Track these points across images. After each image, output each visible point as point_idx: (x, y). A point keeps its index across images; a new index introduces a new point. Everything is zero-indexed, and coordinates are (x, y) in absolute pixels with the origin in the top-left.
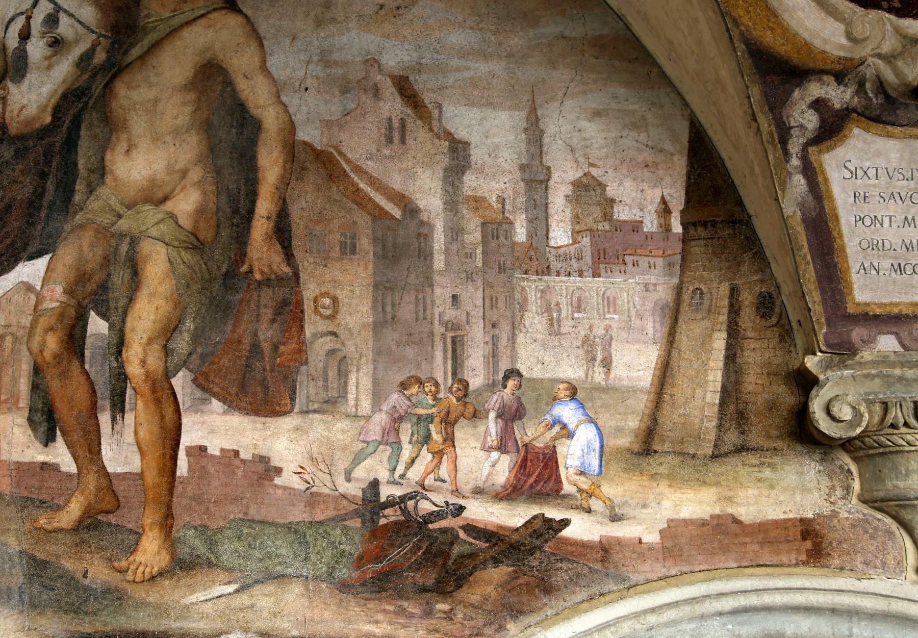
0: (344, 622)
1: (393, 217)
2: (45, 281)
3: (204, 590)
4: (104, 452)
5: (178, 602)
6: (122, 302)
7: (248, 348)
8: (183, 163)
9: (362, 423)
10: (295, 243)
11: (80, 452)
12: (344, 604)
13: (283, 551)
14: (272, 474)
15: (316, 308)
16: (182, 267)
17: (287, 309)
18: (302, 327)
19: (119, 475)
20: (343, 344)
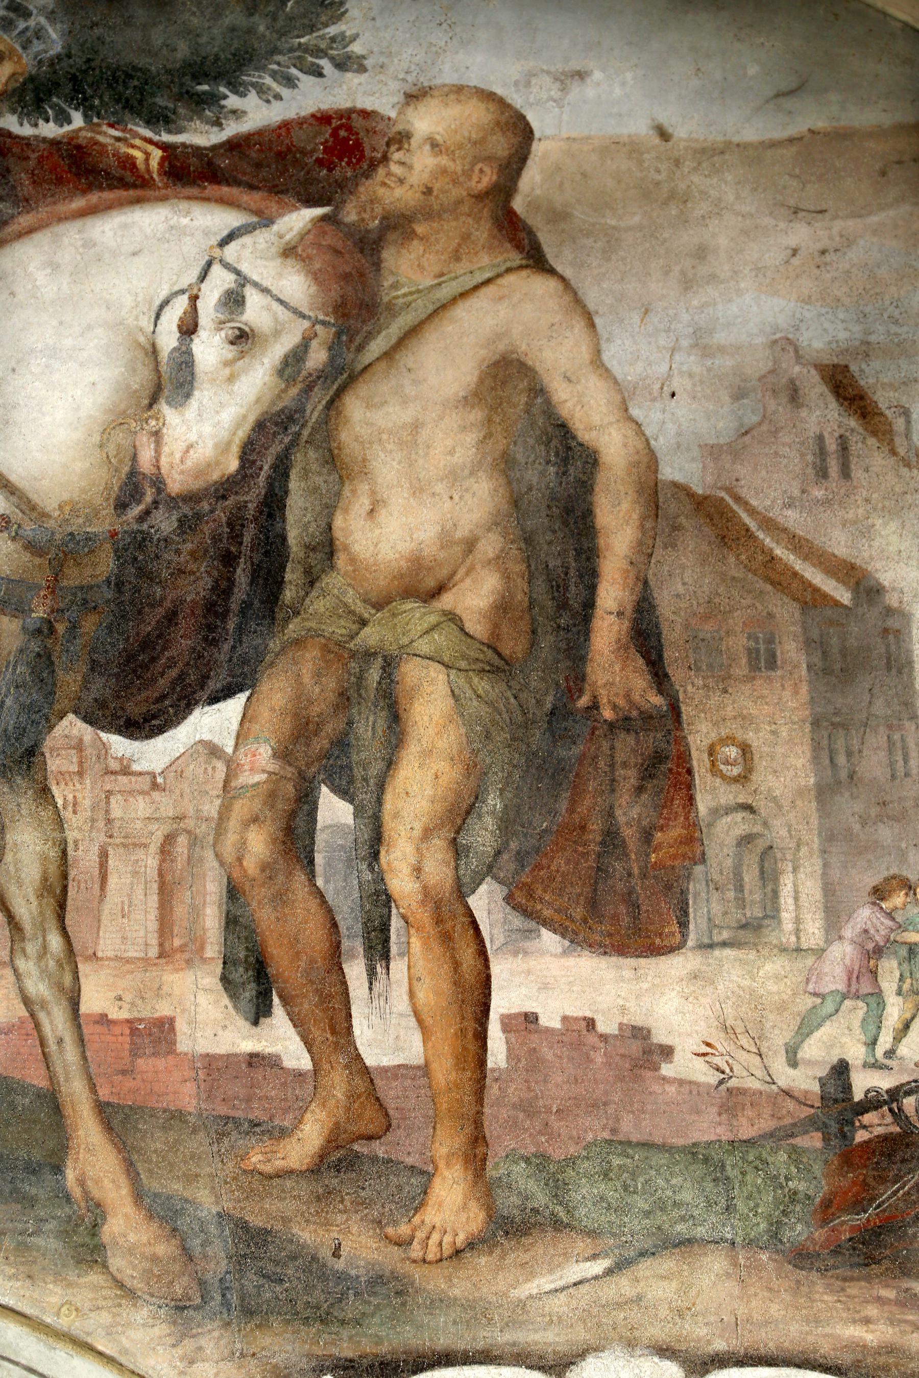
0: (808, 1322)
1: (837, 604)
2: (241, 737)
3: (551, 1271)
4: (357, 1031)
5: (505, 1295)
6: (375, 769)
7: (599, 839)
8: (467, 528)
9: (810, 961)
10: (669, 654)
11: (316, 1033)
12: (804, 1289)
13: (686, 1196)
14: (656, 1058)
15: (713, 764)
16: (475, 703)
17: (663, 767)
18: (691, 799)
19: (385, 1070)
20: (765, 824)
